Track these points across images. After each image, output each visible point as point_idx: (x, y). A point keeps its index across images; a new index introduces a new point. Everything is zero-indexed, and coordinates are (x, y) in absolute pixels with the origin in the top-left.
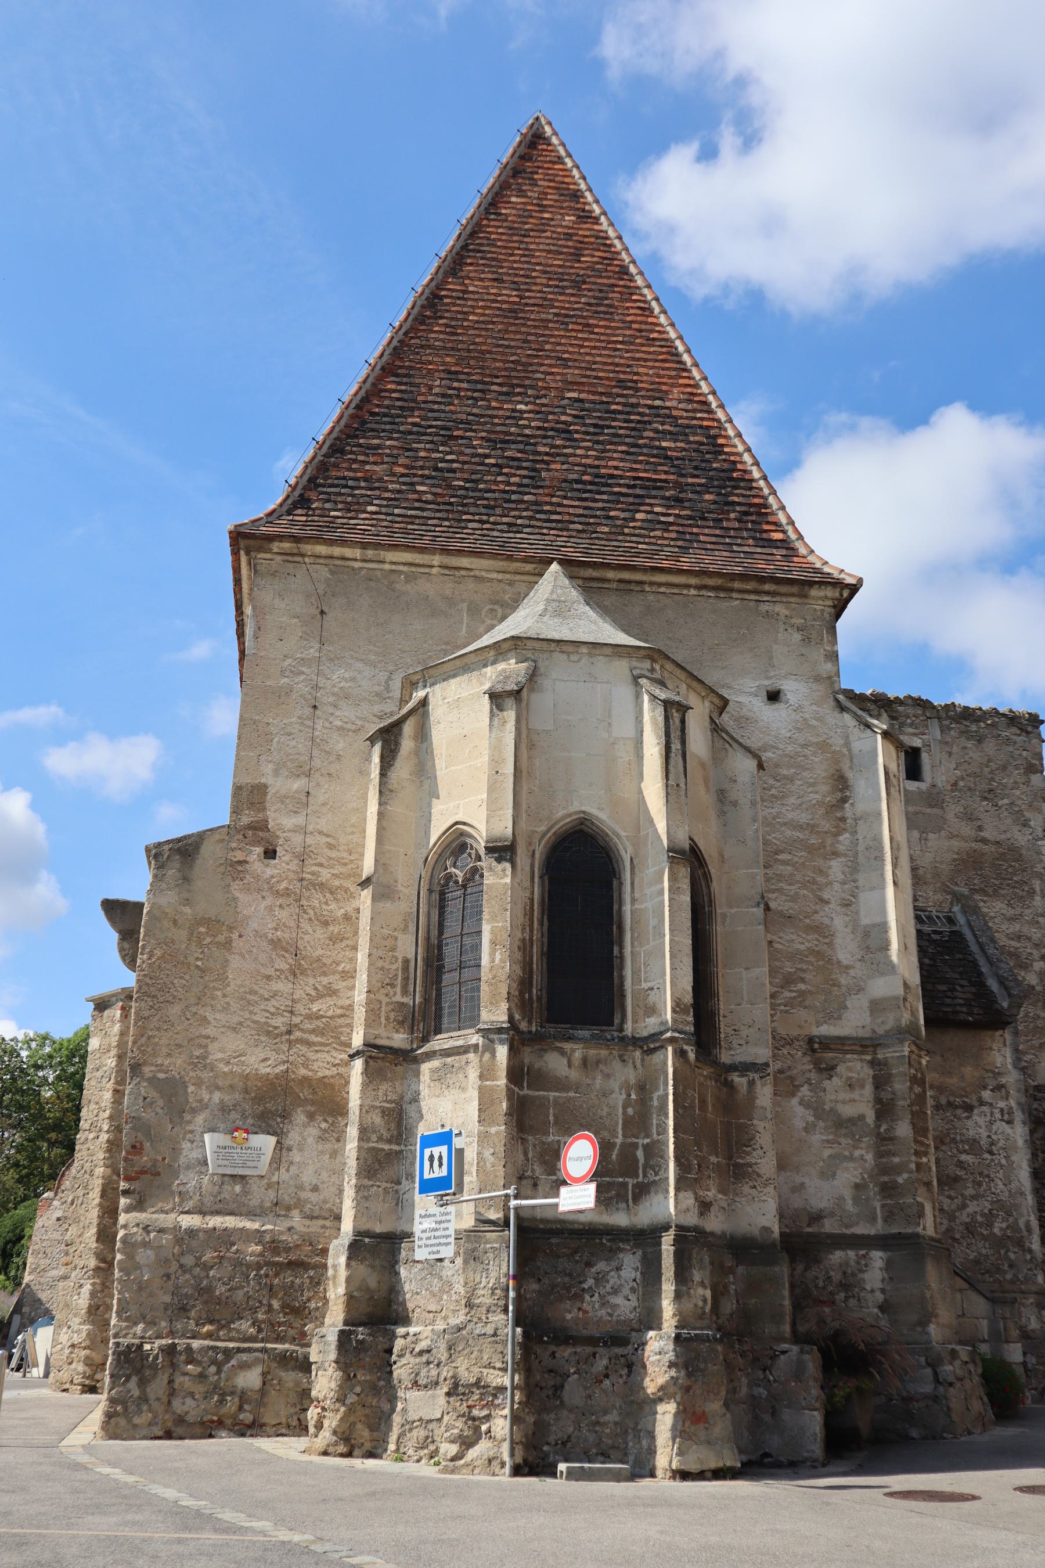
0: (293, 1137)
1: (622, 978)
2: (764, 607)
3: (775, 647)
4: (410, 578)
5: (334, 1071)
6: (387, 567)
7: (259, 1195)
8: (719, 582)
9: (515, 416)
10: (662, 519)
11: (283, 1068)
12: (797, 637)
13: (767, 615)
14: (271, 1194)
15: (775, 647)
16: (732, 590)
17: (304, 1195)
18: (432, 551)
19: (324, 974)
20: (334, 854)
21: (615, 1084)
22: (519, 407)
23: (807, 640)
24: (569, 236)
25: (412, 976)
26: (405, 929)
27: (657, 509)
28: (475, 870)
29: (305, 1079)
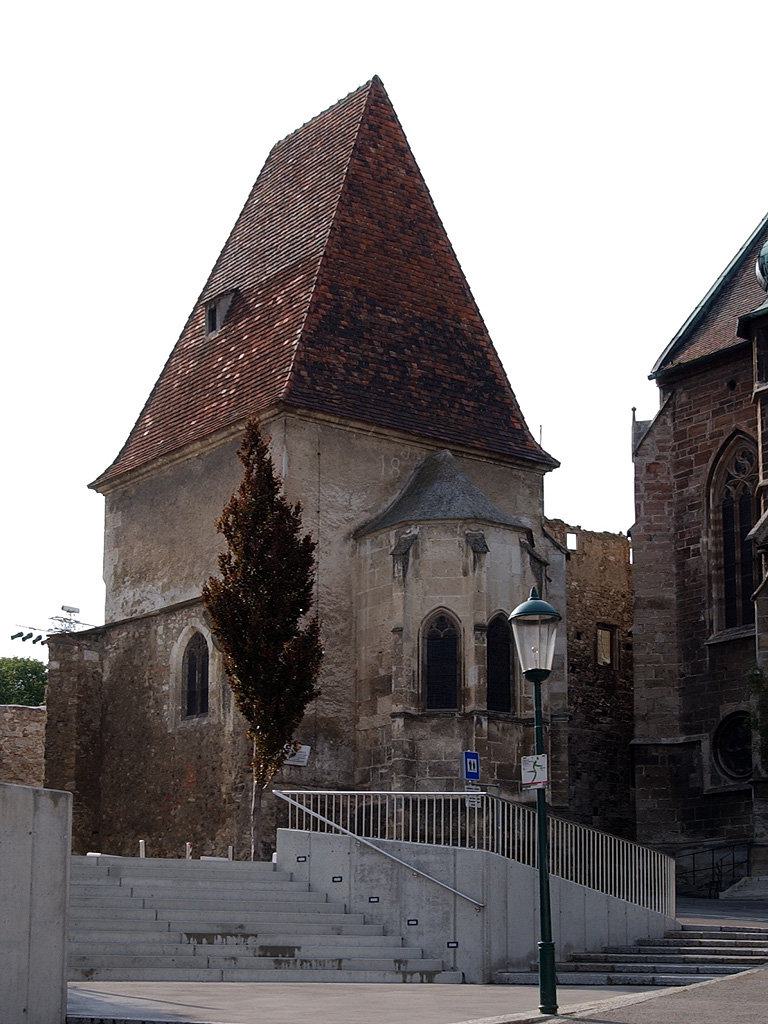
0: (319, 748)
1: (514, 691)
2: (514, 472)
3: (518, 496)
4: (359, 437)
5: (335, 715)
6: (348, 429)
7: (306, 776)
8: (498, 457)
9: (392, 327)
10: (467, 409)
11: (314, 711)
12: (528, 491)
13: (515, 477)
14: (310, 776)
15: (518, 496)
16: (502, 461)
17: (325, 776)
18: (372, 424)
19: (328, 663)
20: (329, 598)
21: (514, 739)
22: (394, 320)
23: (531, 493)
24: (402, 187)
25: (416, 679)
26: (412, 656)
27: (464, 402)
28: (449, 631)
29: (323, 718)
